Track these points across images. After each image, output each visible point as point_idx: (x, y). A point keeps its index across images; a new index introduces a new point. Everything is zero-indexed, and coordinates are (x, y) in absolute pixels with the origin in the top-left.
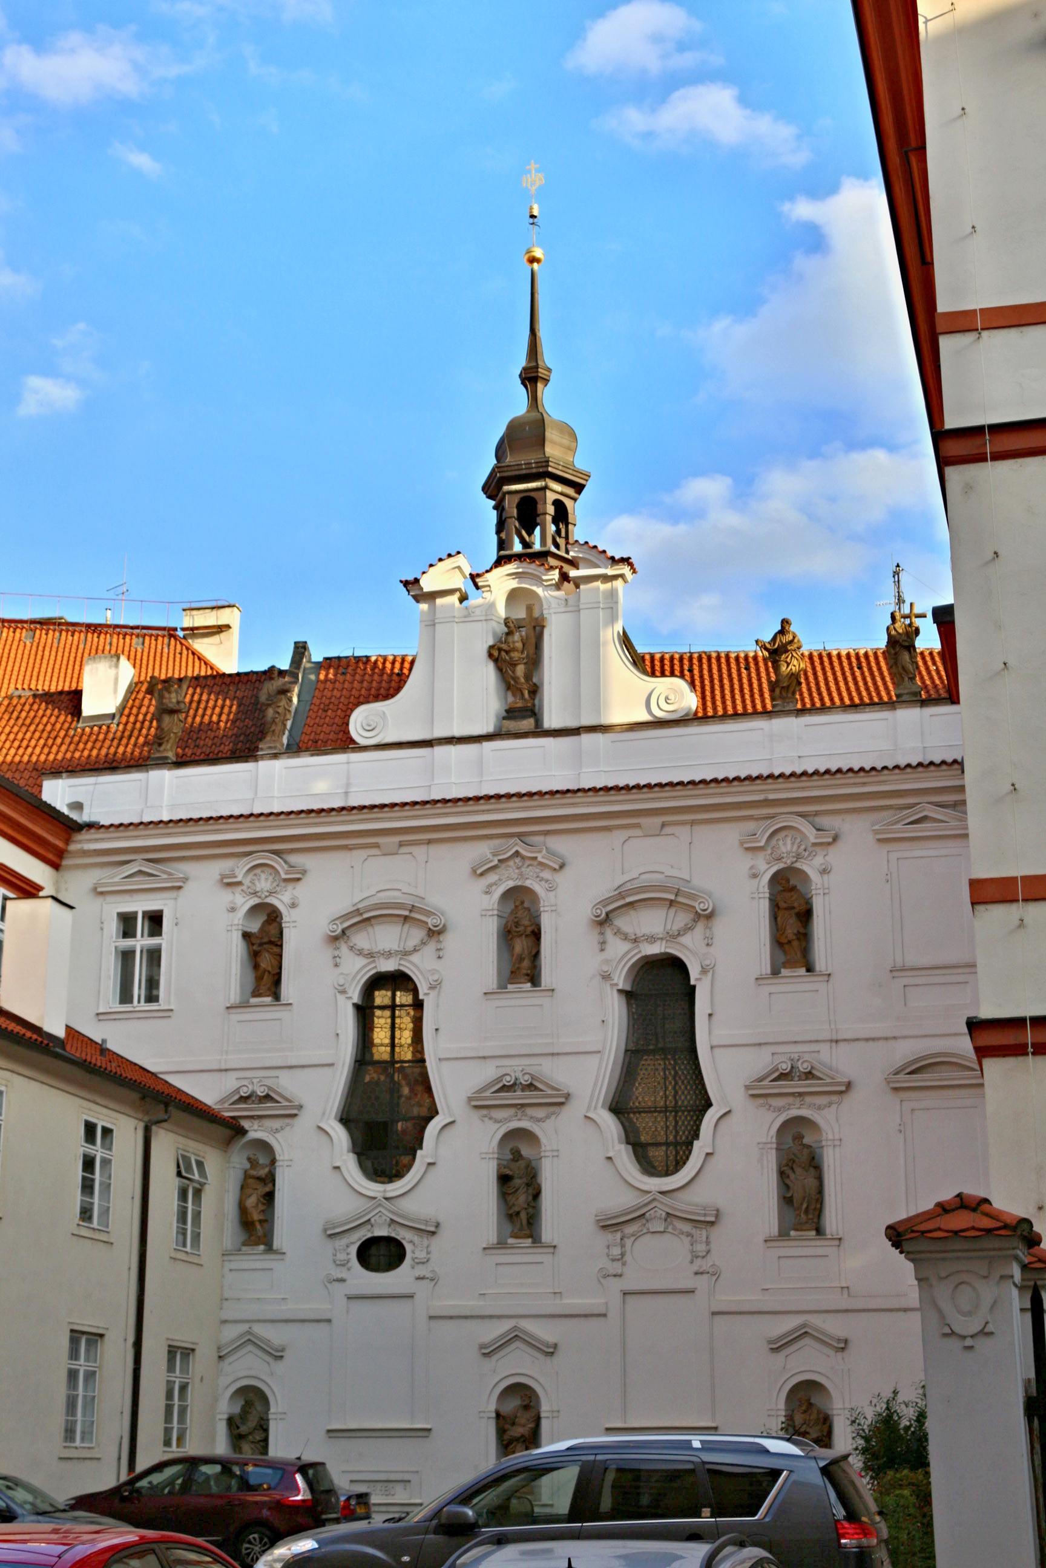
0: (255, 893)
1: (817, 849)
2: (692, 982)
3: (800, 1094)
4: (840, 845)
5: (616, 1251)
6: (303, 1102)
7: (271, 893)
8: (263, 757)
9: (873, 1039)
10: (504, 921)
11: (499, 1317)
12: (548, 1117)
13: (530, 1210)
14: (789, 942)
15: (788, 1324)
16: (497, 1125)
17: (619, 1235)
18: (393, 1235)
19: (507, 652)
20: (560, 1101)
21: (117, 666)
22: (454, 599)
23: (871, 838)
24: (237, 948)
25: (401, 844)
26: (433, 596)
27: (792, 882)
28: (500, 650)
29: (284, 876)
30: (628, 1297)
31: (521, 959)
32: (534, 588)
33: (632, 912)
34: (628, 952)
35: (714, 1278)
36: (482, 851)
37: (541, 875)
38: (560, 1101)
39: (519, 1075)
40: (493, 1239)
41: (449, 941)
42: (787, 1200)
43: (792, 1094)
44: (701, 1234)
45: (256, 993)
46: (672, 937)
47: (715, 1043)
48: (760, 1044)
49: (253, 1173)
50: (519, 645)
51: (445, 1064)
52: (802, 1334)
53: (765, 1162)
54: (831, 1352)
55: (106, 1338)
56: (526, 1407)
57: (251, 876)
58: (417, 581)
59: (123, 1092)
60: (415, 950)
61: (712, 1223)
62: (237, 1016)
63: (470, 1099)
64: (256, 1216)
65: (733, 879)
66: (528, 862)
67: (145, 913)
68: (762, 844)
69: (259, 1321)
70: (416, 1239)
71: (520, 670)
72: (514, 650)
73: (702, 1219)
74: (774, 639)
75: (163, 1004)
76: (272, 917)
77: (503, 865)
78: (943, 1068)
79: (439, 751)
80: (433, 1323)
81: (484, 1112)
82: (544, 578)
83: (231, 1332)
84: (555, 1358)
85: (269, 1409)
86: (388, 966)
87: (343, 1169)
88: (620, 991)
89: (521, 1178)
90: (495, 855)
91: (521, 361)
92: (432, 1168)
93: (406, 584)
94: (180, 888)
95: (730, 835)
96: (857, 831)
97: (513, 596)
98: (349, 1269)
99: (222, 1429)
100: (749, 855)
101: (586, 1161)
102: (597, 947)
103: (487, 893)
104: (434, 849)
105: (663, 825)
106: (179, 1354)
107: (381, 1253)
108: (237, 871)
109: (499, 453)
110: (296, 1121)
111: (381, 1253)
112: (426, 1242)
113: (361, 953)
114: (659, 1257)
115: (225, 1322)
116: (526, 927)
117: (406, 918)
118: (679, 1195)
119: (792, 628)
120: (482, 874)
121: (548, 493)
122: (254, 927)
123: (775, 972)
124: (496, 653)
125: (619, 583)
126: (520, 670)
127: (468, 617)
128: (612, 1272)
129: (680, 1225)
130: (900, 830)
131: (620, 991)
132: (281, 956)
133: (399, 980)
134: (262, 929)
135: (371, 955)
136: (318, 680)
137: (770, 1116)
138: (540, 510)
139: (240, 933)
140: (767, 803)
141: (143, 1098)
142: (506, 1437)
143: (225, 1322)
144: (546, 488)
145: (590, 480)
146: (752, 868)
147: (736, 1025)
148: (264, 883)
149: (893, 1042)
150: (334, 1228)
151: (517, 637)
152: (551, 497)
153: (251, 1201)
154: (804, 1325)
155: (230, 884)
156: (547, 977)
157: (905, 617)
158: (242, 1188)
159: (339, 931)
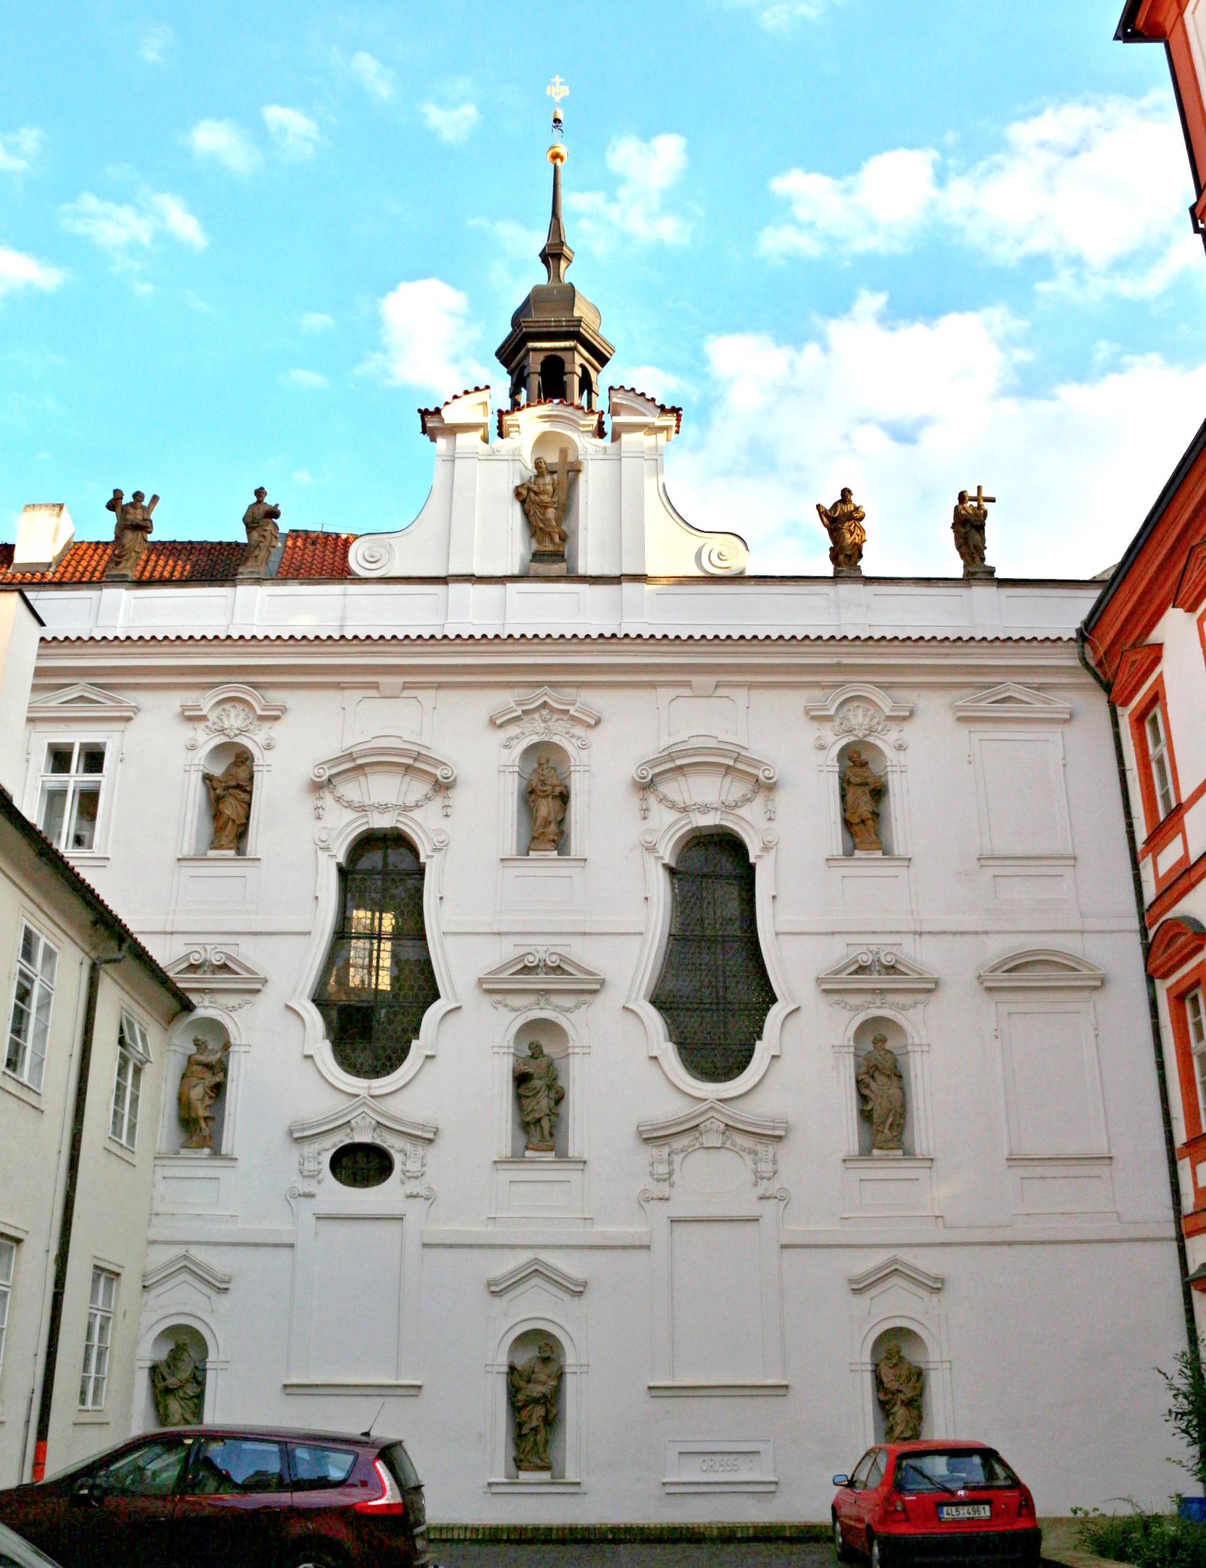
0: (222, 730)
1: (891, 724)
2: (752, 860)
3: (882, 991)
4: (917, 721)
5: (662, 1169)
6: (268, 977)
7: (242, 732)
8: (243, 582)
9: (962, 933)
10: (525, 782)
11: (513, 1247)
12: (577, 1007)
13: (553, 1118)
14: (863, 822)
15: (881, 1257)
16: (514, 1014)
17: (666, 1150)
18: (378, 1142)
19: (536, 493)
20: (591, 988)
21: (59, 515)
22: (476, 436)
23: (949, 717)
24: (196, 793)
25: (406, 686)
26: (453, 430)
27: (864, 757)
28: (529, 490)
29: (260, 712)
30: (675, 1225)
31: (547, 823)
32: (569, 433)
33: (681, 779)
34: (674, 823)
35: (782, 1204)
36: (505, 700)
37: (572, 731)
38: (591, 988)
39: (544, 956)
40: (505, 1149)
41: (459, 797)
42: (866, 1116)
43: (873, 991)
44: (766, 1151)
45: (215, 845)
46: (727, 808)
47: (780, 930)
48: (833, 933)
49: (201, 1058)
50: (550, 488)
51: (449, 939)
52: (892, 1271)
53: (842, 1069)
54: (924, 1294)
55: (25, 1245)
56: (546, 1360)
57: (219, 710)
58: (438, 411)
59: (77, 905)
60: (417, 806)
61: (780, 1138)
62: (188, 870)
63: (481, 981)
64: (202, 1112)
65: (795, 747)
66: (556, 717)
67: (83, 745)
68: (832, 712)
69: (199, 1243)
70: (409, 1147)
71: (551, 513)
72: (544, 492)
73: (770, 1132)
74: (835, 506)
75: (97, 851)
76: (242, 758)
77: (526, 718)
78: (1039, 967)
79: (454, 588)
80: (430, 1253)
81: (498, 997)
82: (582, 422)
83: (161, 1257)
84: (585, 1297)
85: (206, 1356)
86: (382, 822)
87: (317, 1059)
88: (665, 866)
89: (541, 1079)
90: (519, 704)
91: (540, 240)
92: (430, 1063)
93: (424, 413)
94: (129, 719)
95: (795, 701)
96: (934, 709)
97: (543, 441)
98: (319, 1182)
99: (142, 1382)
100: (816, 725)
101: (623, 1060)
102: (639, 814)
103: (506, 746)
104: (446, 696)
105: (717, 686)
106: (105, 1275)
107: (362, 1164)
108: (202, 702)
109: (516, 322)
110: (259, 998)
111: (362, 1164)
112: (420, 1152)
113: (349, 805)
114: (714, 1178)
115: (154, 1242)
116: (554, 787)
117: (408, 767)
118: (739, 1103)
119: (853, 498)
120: (501, 726)
121: (576, 355)
122: (218, 771)
123: (848, 854)
124: (525, 492)
125: (662, 437)
126: (551, 513)
127: (492, 457)
128: (656, 1194)
129: (741, 1141)
130: (986, 708)
131: (665, 866)
132: (249, 805)
133: (397, 840)
134: (228, 772)
135: (362, 809)
136: (286, 546)
137: (846, 1015)
138: (568, 368)
139: (200, 774)
140: (839, 668)
141: (94, 924)
142: (520, 1397)
143: (154, 1242)
144: (573, 349)
145: (615, 355)
146: (819, 738)
147: (804, 910)
148: (234, 719)
149: (982, 938)
150: (303, 1130)
151: (548, 479)
152: (579, 360)
153: (196, 1093)
154: (895, 1261)
155: (192, 718)
156: (577, 843)
157: (972, 499)
158: (184, 1077)
159: (325, 777)
